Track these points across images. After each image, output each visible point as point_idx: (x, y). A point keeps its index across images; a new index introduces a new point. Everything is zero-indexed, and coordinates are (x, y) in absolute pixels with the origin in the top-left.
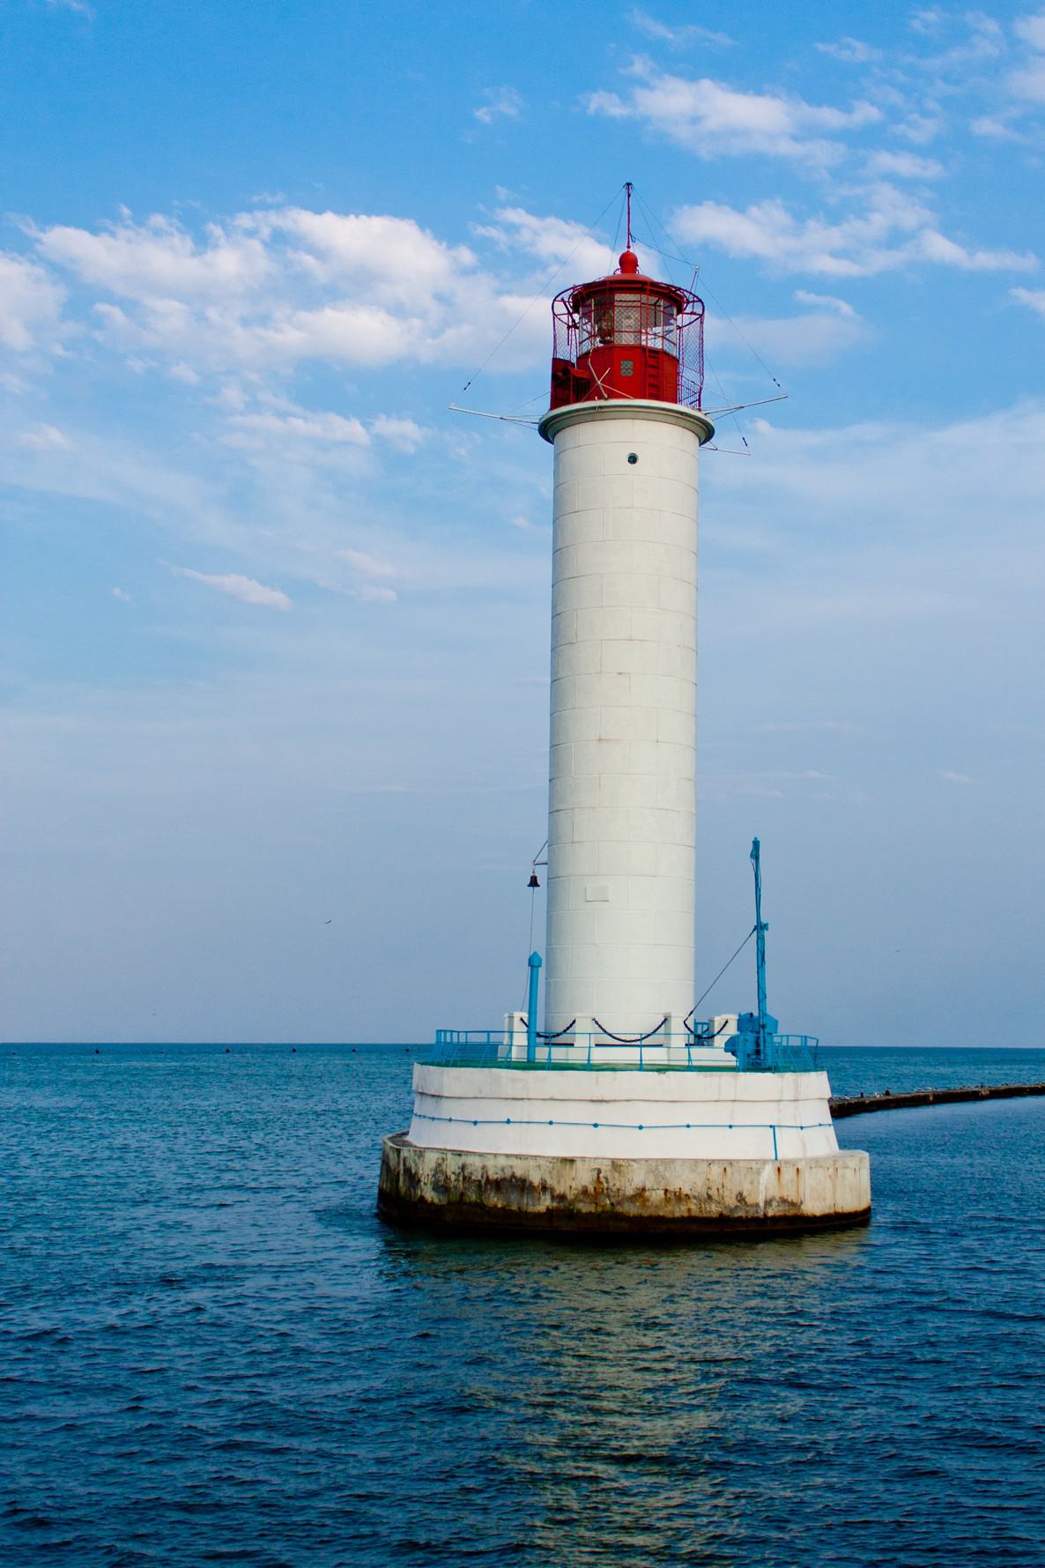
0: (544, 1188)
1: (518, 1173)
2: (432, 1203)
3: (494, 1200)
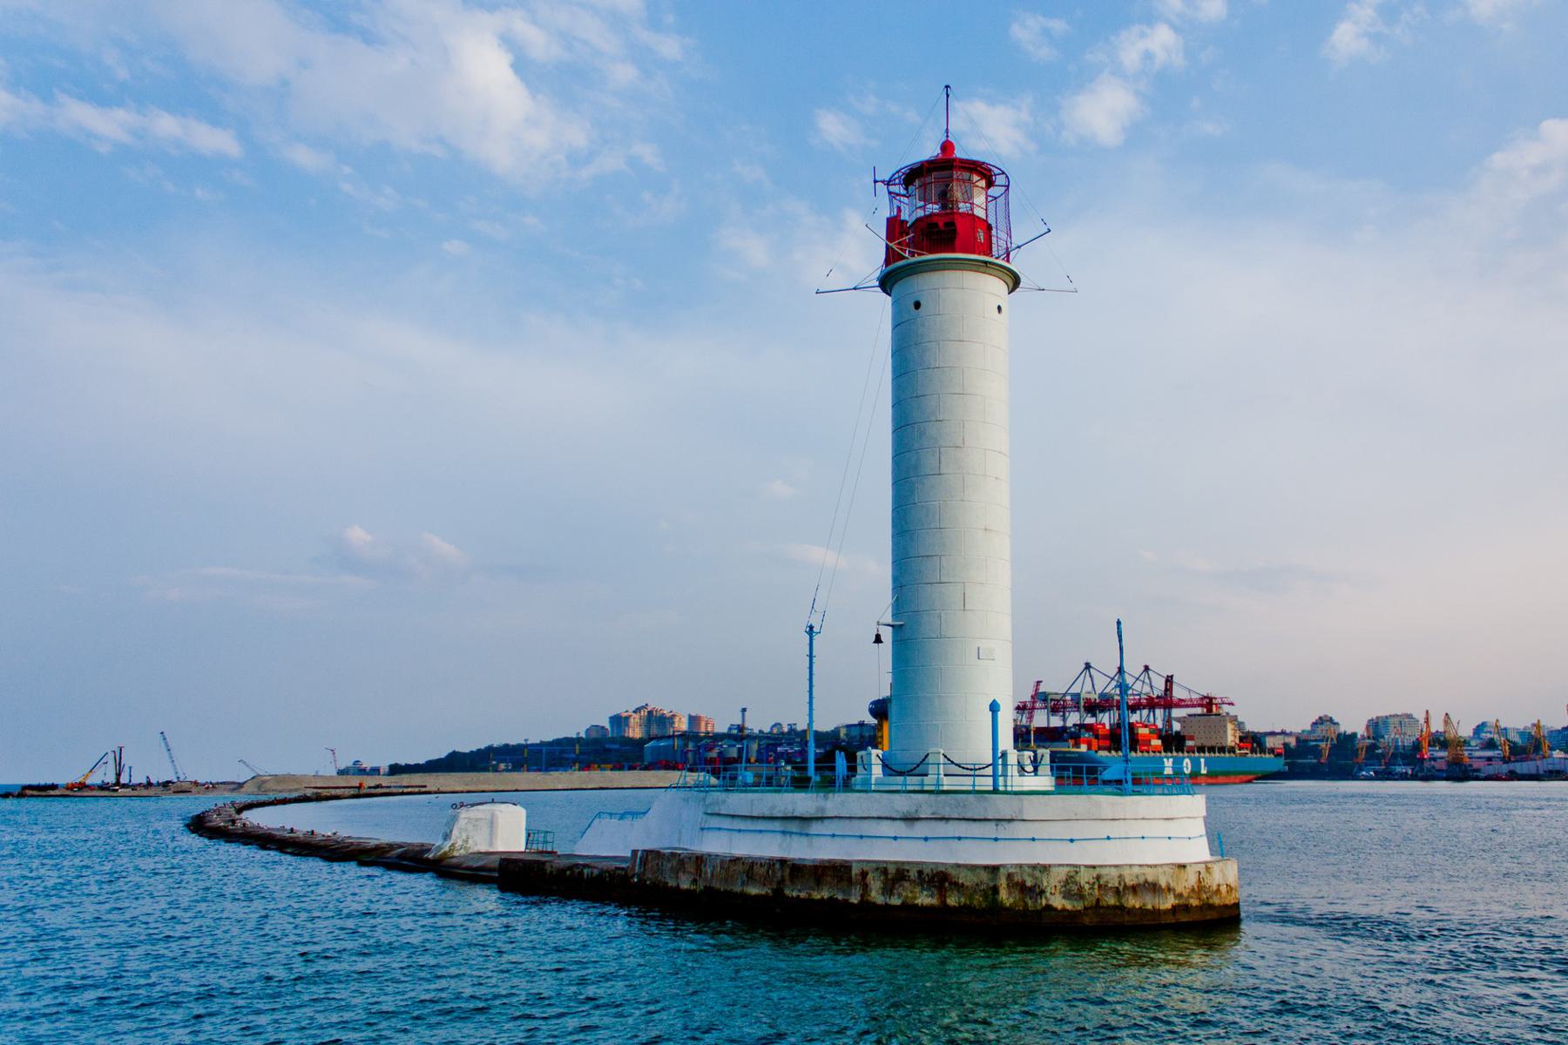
0: (1169, 889)
1: (1150, 879)
2: (1064, 910)
3: (1132, 902)
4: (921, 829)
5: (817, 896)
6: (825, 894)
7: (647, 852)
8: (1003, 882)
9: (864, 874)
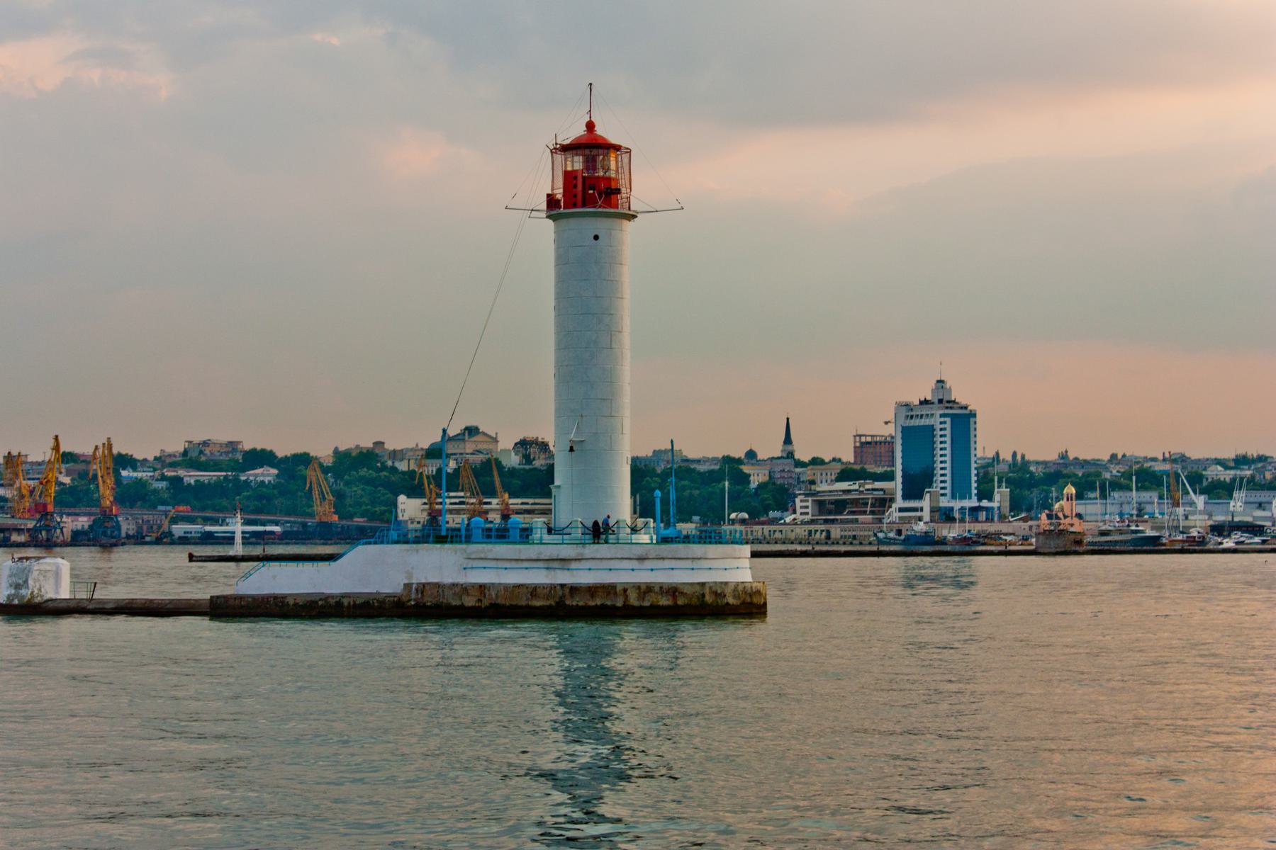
3: (755, 600)
4: (648, 564)
5: (592, 603)
6: (598, 602)
7: (424, 585)
8: (707, 591)
9: (625, 590)
